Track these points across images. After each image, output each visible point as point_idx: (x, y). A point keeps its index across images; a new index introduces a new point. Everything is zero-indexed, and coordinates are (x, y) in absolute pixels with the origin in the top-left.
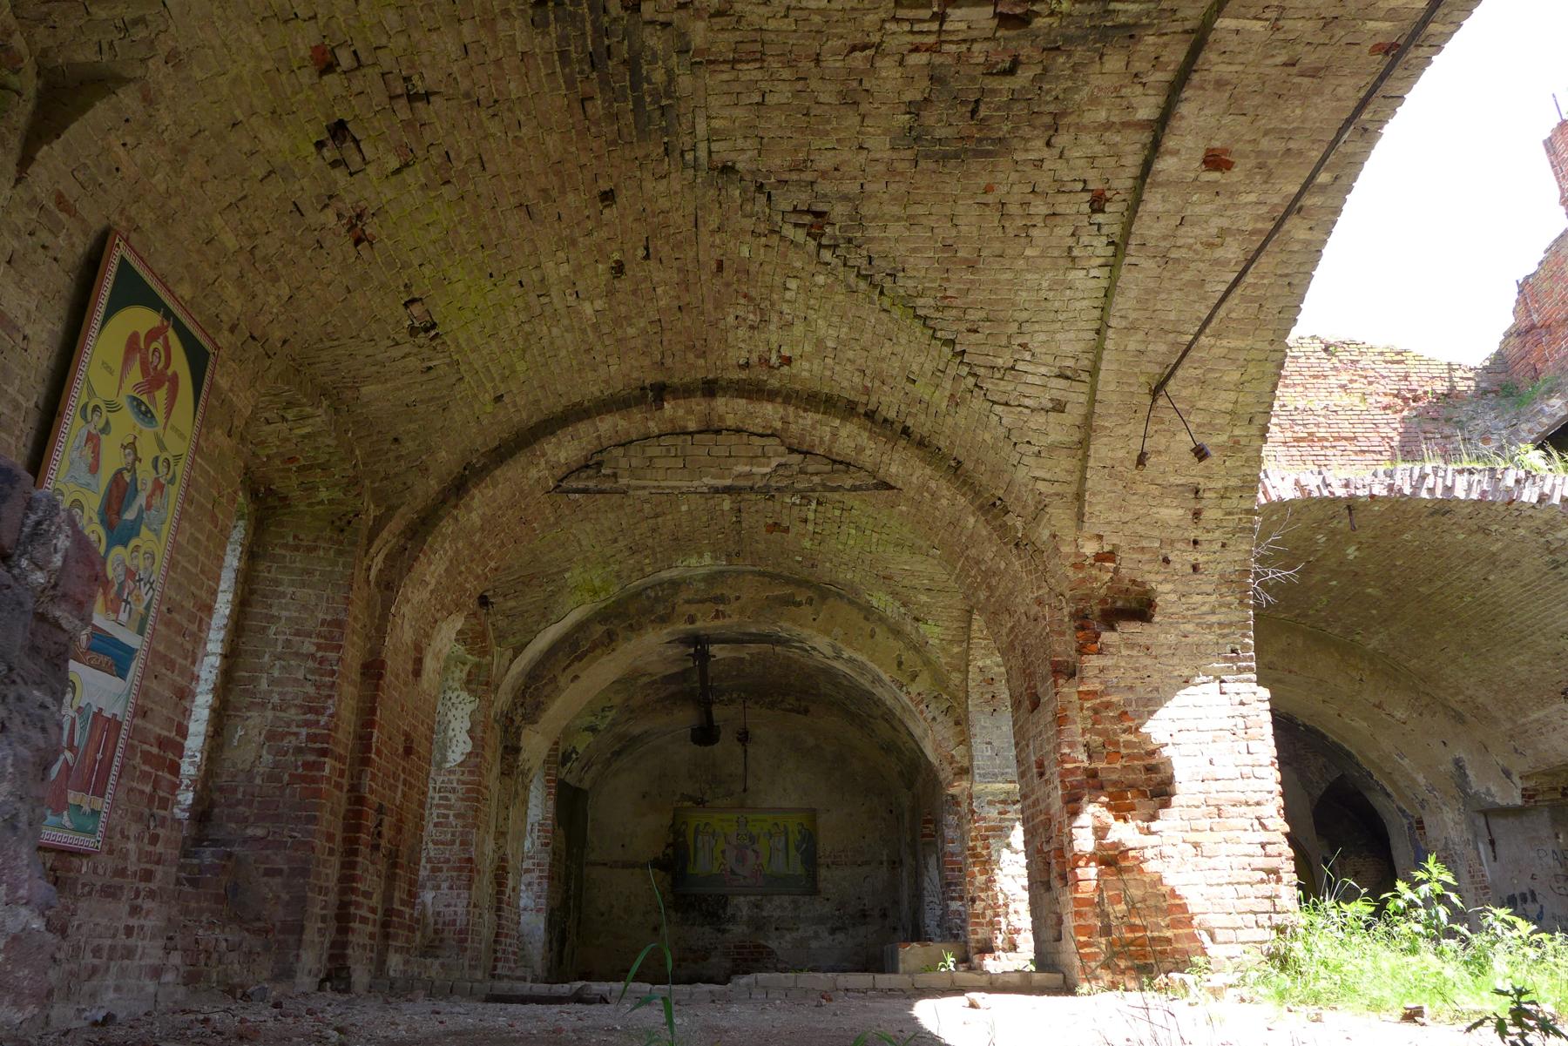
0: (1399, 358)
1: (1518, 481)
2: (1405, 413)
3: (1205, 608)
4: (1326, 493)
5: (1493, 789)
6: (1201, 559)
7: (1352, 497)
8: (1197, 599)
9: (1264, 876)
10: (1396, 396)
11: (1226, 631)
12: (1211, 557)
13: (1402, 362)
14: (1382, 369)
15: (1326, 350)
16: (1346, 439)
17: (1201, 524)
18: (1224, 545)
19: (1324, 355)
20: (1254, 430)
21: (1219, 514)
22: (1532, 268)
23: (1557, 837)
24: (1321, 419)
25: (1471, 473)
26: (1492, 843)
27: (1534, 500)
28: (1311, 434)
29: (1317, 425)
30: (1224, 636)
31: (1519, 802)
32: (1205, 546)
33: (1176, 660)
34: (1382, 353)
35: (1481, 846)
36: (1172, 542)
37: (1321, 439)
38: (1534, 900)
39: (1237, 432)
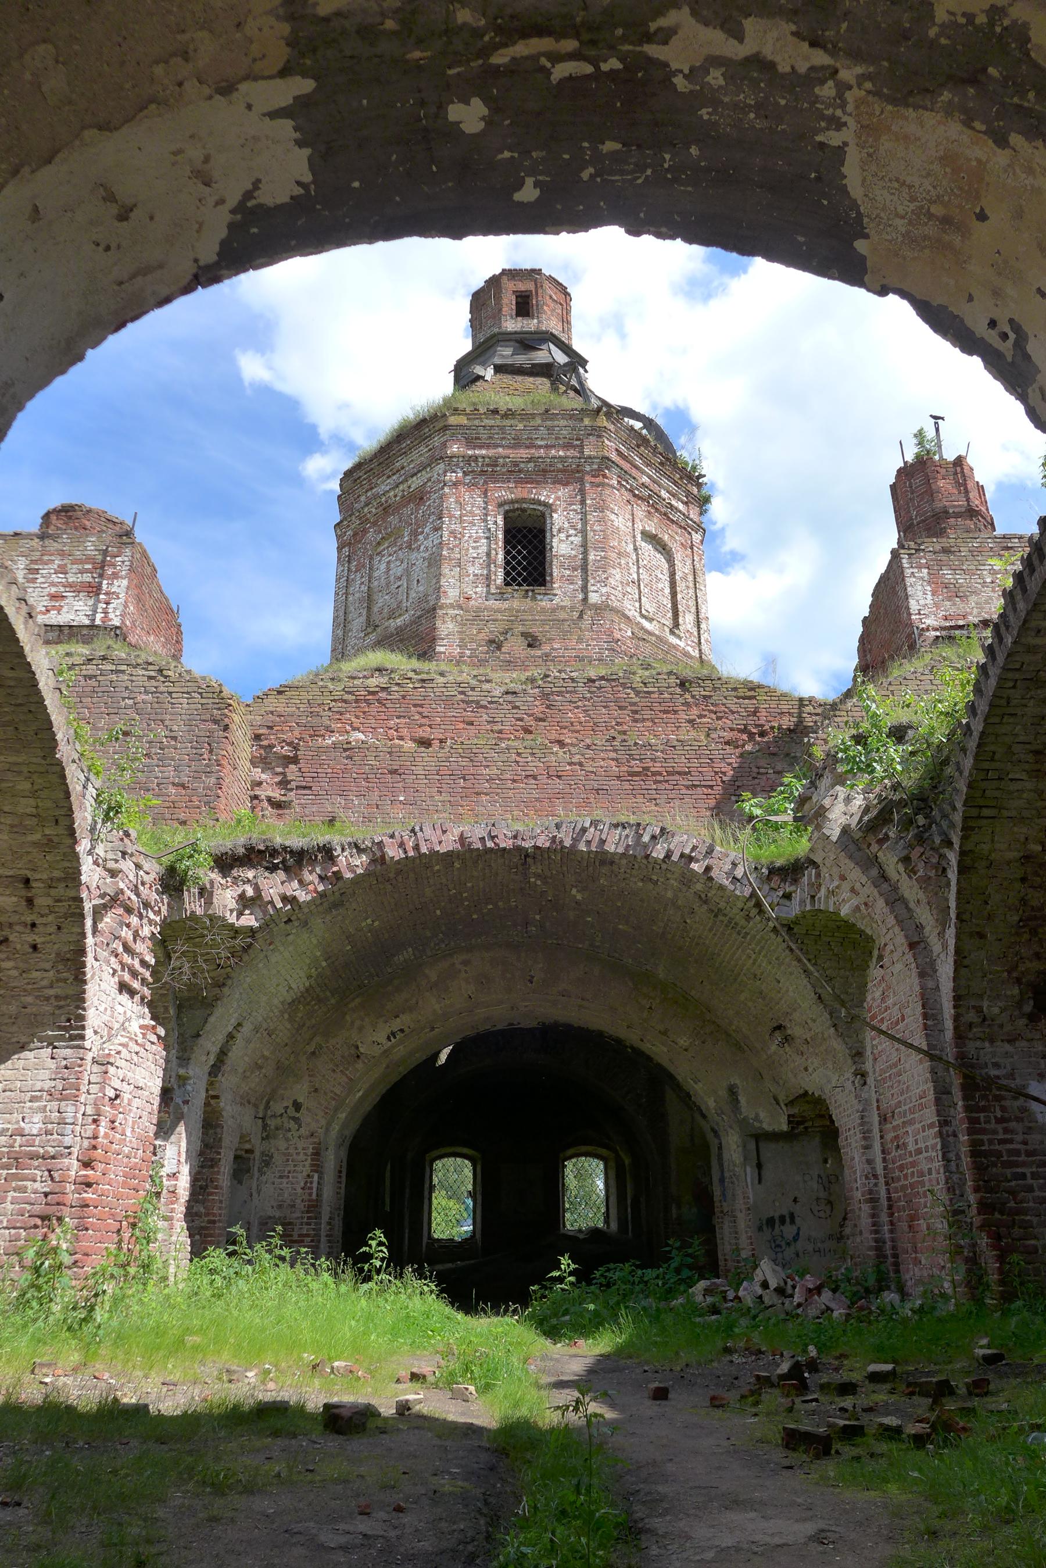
0: (752, 693)
1: (654, 837)
2: (748, 747)
3: (45, 983)
4: (490, 844)
5: (762, 1115)
6: (39, 940)
7: (518, 849)
8: (35, 974)
9: (39, 1222)
10: (740, 731)
11: (62, 1003)
12: (48, 938)
13: (754, 697)
14: (732, 704)
15: (682, 685)
16: (679, 773)
17: (36, 909)
18: (59, 928)
19: (678, 690)
20: (61, 830)
21: (49, 901)
22: (866, 613)
23: (826, 1161)
25: (624, 828)
26: (759, 1166)
27: (661, 856)
29: (653, 760)
30: (60, 1007)
31: (785, 1127)
32: (40, 929)
33: (14, 1029)
34: (735, 689)
35: (748, 1169)
36: (11, 925)
37: (654, 774)
38: (793, 1221)
39: (47, 832)
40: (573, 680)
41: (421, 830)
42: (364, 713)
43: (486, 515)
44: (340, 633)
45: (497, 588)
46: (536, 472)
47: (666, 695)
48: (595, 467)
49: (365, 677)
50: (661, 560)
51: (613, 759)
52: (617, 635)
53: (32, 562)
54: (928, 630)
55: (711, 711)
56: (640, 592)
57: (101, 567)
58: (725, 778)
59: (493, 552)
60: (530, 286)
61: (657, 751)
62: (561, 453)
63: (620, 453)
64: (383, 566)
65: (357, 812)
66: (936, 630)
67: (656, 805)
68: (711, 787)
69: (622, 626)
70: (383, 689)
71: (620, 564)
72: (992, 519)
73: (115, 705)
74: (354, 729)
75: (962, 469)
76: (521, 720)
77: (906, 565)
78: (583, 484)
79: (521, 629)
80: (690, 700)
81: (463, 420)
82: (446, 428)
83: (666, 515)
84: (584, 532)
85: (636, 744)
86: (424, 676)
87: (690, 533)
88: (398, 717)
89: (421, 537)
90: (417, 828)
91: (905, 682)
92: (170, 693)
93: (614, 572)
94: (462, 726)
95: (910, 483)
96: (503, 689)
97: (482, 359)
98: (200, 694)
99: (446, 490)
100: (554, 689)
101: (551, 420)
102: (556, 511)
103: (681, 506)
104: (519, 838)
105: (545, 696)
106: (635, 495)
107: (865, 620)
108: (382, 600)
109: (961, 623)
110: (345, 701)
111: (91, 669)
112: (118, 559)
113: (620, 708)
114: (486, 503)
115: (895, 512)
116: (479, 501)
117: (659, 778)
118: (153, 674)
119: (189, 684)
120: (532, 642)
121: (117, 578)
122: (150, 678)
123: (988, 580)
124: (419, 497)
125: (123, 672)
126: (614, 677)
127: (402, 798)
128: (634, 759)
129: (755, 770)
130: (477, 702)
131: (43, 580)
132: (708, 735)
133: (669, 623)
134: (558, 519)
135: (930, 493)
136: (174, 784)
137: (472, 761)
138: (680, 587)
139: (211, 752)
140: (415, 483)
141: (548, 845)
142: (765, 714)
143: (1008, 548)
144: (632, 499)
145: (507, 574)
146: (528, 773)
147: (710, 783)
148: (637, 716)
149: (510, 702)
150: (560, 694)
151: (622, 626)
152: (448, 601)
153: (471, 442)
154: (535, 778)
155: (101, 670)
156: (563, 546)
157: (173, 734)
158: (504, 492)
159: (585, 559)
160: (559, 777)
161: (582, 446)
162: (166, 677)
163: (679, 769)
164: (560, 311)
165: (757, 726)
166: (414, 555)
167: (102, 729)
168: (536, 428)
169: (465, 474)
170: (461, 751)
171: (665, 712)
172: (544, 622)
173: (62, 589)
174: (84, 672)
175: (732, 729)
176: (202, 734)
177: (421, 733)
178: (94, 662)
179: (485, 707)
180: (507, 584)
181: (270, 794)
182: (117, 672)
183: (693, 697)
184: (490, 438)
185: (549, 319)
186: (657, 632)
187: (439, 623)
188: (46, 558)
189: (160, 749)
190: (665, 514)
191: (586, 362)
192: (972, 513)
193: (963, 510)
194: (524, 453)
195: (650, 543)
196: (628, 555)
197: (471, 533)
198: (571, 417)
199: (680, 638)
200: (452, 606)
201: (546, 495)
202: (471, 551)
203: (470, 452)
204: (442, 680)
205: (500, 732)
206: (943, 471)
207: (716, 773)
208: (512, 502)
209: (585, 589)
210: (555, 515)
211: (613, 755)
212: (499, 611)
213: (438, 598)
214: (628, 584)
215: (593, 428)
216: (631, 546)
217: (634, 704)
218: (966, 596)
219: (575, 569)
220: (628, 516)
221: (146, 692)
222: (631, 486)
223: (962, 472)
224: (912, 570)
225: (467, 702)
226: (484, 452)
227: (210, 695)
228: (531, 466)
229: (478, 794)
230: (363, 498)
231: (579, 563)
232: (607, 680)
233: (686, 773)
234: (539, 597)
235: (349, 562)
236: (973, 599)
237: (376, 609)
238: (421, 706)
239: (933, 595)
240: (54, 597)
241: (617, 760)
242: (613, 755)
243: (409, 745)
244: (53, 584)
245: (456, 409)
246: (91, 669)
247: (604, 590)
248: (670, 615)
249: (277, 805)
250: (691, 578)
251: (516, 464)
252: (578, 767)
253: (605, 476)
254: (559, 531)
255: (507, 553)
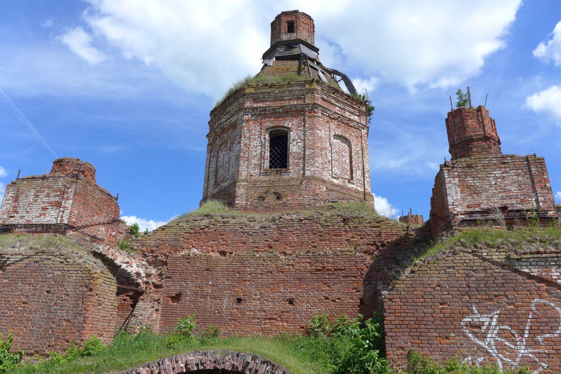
0: (378, 225)
2: (376, 253)
4: (201, 367)
7: (216, 369)
10: (372, 245)
13: (379, 227)
19: (342, 224)
24: (331, 260)
28: (324, 267)
34: (370, 223)
37: (328, 270)
40: (292, 220)
41: (163, 363)
42: (198, 239)
43: (261, 135)
44: (206, 185)
45: (264, 170)
46: (284, 113)
47: (336, 227)
48: (310, 108)
49: (200, 220)
50: (346, 146)
51: (308, 263)
52: (317, 192)
53: (37, 192)
54: (458, 215)
55: (358, 235)
56: (332, 166)
57: (63, 193)
58: (362, 272)
59: (263, 153)
60: (294, 18)
61: (329, 258)
62: (295, 103)
63: (323, 99)
64: (222, 156)
65: (191, 290)
66: (462, 214)
67: (329, 286)
68: (355, 277)
69: (321, 186)
70: (207, 227)
71: (321, 154)
72: (499, 139)
73: (45, 277)
74: (193, 247)
75: (481, 113)
76: (267, 241)
77: (446, 177)
78: (304, 117)
79: (273, 190)
80: (348, 229)
81: (252, 90)
82: (244, 95)
83: (348, 123)
84: (304, 140)
85: (319, 254)
86: (225, 220)
87: (360, 130)
88: (213, 241)
89: (234, 145)
90: (161, 363)
91: (437, 262)
92: (68, 271)
93: (318, 159)
94: (241, 244)
95: (454, 121)
96: (260, 225)
97: (269, 56)
98: (81, 271)
99: (244, 124)
100: (283, 225)
101: (291, 87)
102: (291, 131)
103: (356, 118)
104: (217, 363)
105: (279, 229)
106: (331, 118)
107: (433, 189)
108: (221, 172)
109: (477, 209)
110: (190, 233)
111: (37, 258)
112: (70, 190)
113: (314, 234)
114: (261, 129)
115: (448, 134)
116: (258, 128)
117: (330, 272)
118: (62, 260)
119: (77, 266)
120: (279, 197)
121: (68, 199)
122: (61, 262)
123: (493, 183)
124: (234, 126)
125: (50, 259)
126: (312, 218)
127: (210, 283)
128: (318, 263)
129: (378, 267)
130: (248, 233)
131: (39, 200)
132: (355, 248)
133: (348, 177)
134: (292, 135)
135: (464, 128)
136: (65, 320)
137: (243, 264)
138: (354, 157)
139: (83, 303)
140: (233, 119)
141: (230, 369)
142: (384, 235)
143: (505, 163)
144: (329, 120)
145: (270, 162)
146: (268, 270)
147: (355, 275)
148: (322, 238)
149: (263, 232)
150: (286, 227)
151: (321, 186)
152: (242, 178)
153: (256, 100)
154: (271, 272)
155: (40, 258)
156: (295, 148)
157: (67, 293)
158: (269, 123)
159: (304, 154)
160: (282, 272)
161: (304, 98)
162: (68, 262)
163: (340, 268)
164: (307, 28)
165: (380, 242)
166: (232, 154)
167: (38, 289)
168: (284, 92)
169: (252, 115)
170: (238, 259)
171: (336, 236)
172: (284, 187)
173: (47, 205)
174: (34, 260)
175: (368, 244)
176: (80, 293)
177: (222, 248)
178: (39, 254)
179: (251, 235)
180: (271, 167)
181: (154, 280)
182: (48, 259)
183: (349, 227)
184: (264, 98)
185: (302, 32)
186: (341, 184)
187: (237, 189)
188: (42, 189)
189: (62, 301)
190: (347, 124)
191: (318, 50)
192: (486, 138)
193: (482, 137)
194: (278, 104)
195: (340, 139)
196: (326, 148)
197: (254, 143)
198: (300, 85)
199: (353, 184)
200: (243, 181)
201: (288, 123)
202: (254, 152)
203: (255, 105)
204: (233, 221)
205: (257, 247)
206: (471, 115)
207: (358, 269)
208: (273, 127)
209: (304, 169)
210: (291, 133)
211: (308, 260)
212: (264, 182)
213: (238, 176)
214: (326, 163)
215: (310, 90)
216: (329, 144)
217: (320, 232)
218: (480, 193)
219: (300, 159)
220: (327, 129)
221: (59, 270)
222: (329, 114)
223: (481, 115)
224: (449, 179)
225: (244, 233)
226: (261, 105)
227: (86, 272)
228: (281, 110)
229: (245, 281)
230: (217, 124)
231: (302, 156)
232: (308, 220)
233: (343, 270)
234: (283, 174)
235: (211, 153)
236: (485, 194)
237: (219, 176)
238: (223, 235)
239: (461, 193)
240: (44, 209)
241: (310, 263)
242: (308, 260)
243: (215, 255)
244: (44, 203)
245: (249, 86)
246: (37, 258)
247: (312, 169)
248: (349, 173)
249: (156, 286)
250: (360, 152)
251: (274, 110)
252: (291, 267)
253: (315, 112)
254: (293, 140)
255: (271, 151)
